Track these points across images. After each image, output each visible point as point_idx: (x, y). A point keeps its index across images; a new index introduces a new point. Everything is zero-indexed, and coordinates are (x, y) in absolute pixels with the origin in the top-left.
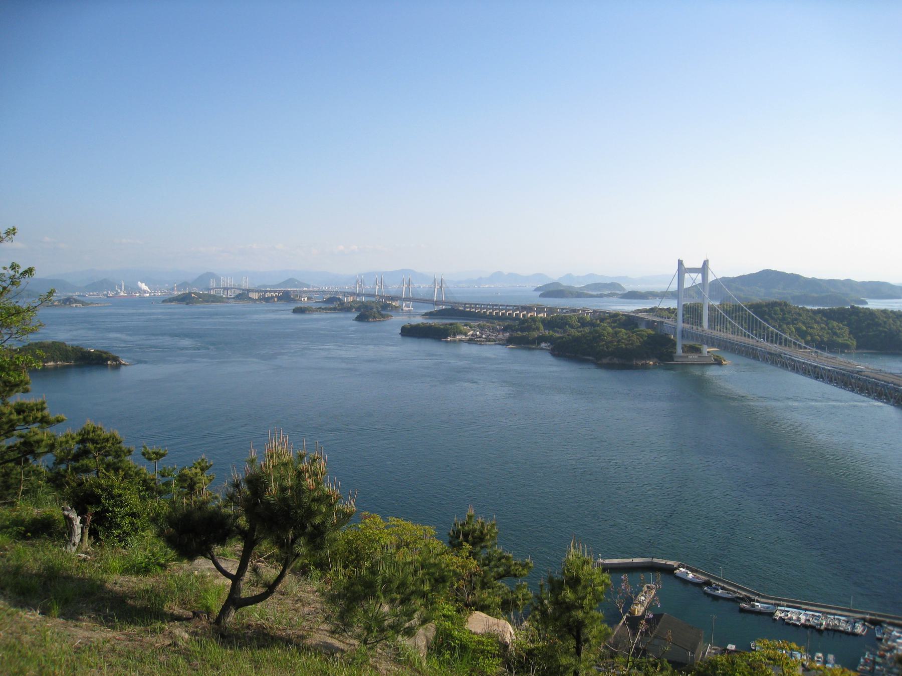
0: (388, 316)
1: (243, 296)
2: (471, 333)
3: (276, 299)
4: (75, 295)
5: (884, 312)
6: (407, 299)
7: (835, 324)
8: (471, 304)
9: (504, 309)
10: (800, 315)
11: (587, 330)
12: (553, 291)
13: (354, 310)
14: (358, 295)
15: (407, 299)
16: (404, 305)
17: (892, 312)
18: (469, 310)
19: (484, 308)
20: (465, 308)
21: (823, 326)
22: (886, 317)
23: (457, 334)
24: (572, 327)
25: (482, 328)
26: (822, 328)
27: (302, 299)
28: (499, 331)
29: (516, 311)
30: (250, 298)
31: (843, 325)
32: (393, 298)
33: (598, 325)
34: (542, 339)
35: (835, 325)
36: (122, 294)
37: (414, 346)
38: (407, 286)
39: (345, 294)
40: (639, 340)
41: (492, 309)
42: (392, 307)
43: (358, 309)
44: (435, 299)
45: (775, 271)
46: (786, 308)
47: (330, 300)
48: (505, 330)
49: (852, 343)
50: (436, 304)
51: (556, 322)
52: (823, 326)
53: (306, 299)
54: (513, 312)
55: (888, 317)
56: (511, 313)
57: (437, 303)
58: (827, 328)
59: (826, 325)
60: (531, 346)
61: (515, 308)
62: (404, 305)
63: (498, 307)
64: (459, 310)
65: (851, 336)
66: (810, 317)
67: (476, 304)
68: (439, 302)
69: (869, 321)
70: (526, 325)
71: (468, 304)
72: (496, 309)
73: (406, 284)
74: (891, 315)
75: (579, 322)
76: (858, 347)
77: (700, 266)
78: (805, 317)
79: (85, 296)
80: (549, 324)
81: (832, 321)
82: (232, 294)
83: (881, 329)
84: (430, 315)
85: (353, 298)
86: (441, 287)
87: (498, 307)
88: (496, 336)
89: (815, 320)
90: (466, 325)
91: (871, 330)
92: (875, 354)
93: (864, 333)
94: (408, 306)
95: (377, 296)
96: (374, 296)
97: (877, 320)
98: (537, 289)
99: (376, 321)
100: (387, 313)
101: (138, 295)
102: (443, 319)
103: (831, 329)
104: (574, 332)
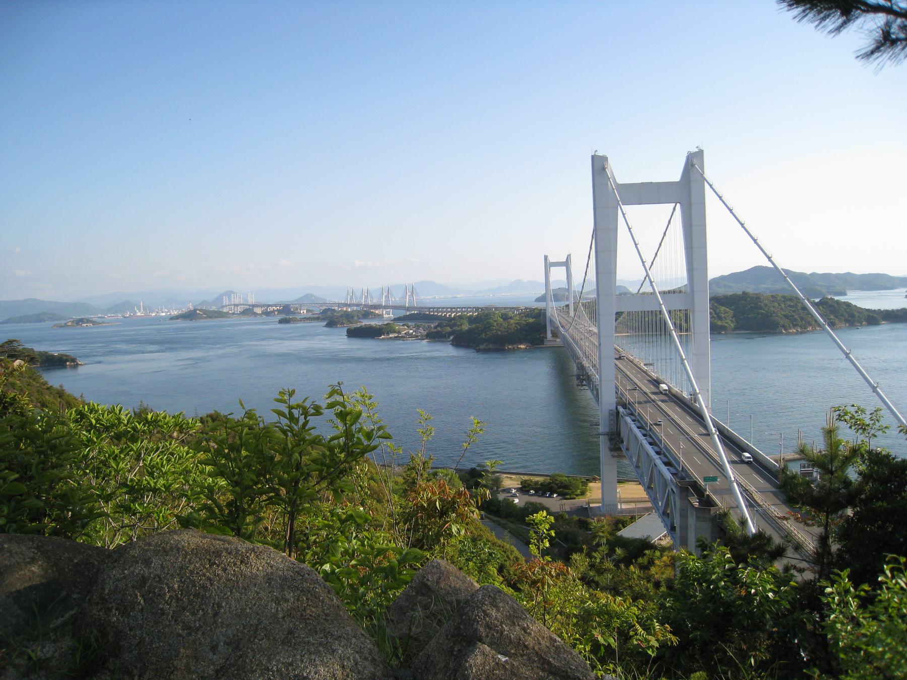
1: (248, 312)
3: (276, 313)
4: (93, 317)
6: (386, 307)
15: (386, 307)
16: (384, 312)
27: (302, 312)
30: (255, 314)
36: (139, 314)
39: (339, 305)
42: (375, 316)
47: (325, 311)
53: (305, 311)
62: (384, 312)
76: (736, 329)
79: (104, 318)
82: (240, 309)
92: (752, 333)
94: (388, 313)
101: (154, 314)
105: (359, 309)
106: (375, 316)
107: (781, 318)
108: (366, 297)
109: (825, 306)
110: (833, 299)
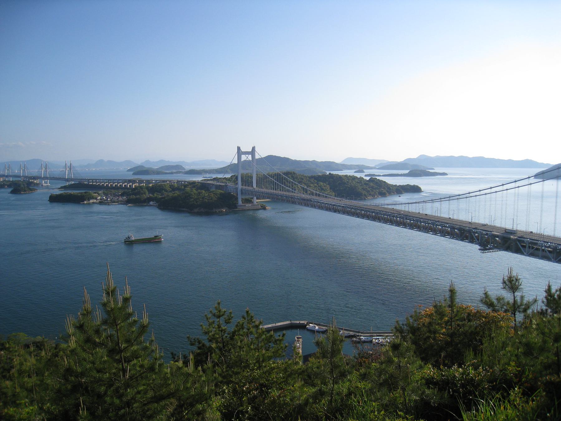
0: (34, 190)
2: (99, 198)
5: (346, 176)
6: (45, 178)
7: (322, 183)
8: (93, 180)
9: (112, 182)
10: (303, 179)
11: (177, 193)
12: (141, 170)
13: (6, 187)
14: (7, 176)
15: (45, 178)
16: (43, 182)
17: (349, 176)
18: (91, 183)
19: (102, 182)
20: (89, 182)
21: (316, 185)
22: (347, 179)
23: (91, 199)
24: (166, 191)
25: (106, 195)
26: (315, 186)
28: (118, 196)
29: (120, 183)
31: (326, 184)
32: (35, 178)
33: (184, 190)
34: (149, 199)
35: (322, 184)
37: (60, 210)
38: (44, 169)
40: (215, 196)
41: (108, 182)
43: (9, 186)
44: (67, 177)
45: (275, 156)
46: (295, 175)
48: (122, 195)
49: (333, 194)
50: (67, 181)
51: (157, 188)
52: (316, 185)
54: (123, 184)
55: (349, 179)
56: (126, 185)
57: (68, 180)
58: (318, 186)
59: (317, 185)
60: (143, 204)
61: (124, 181)
62: (43, 182)
63: (112, 181)
64: (85, 184)
65: (331, 190)
66: (308, 180)
67: (96, 180)
68: (69, 179)
69: (340, 182)
70: (136, 191)
71: (91, 180)
72: (111, 183)
73: (44, 167)
74: (350, 178)
75: (170, 188)
77: (251, 150)
78: (305, 181)
80: (152, 190)
81: (320, 182)
83: (346, 185)
84: (65, 188)
85: (3, 179)
86: (70, 169)
87: (112, 181)
88: (117, 199)
89: (311, 182)
90: (95, 193)
91: (341, 187)
93: (338, 188)
95: (22, 176)
96: (19, 177)
97: (343, 181)
98: (129, 170)
99: (26, 193)
100: (33, 187)
102: (79, 190)
103: (320, 187)
104: (171, 194)
105: (19, 179)
106: (34, 184)
107: (361, 190)
108: (24, 171)
109: (374, 183)
110: (376, 178)
